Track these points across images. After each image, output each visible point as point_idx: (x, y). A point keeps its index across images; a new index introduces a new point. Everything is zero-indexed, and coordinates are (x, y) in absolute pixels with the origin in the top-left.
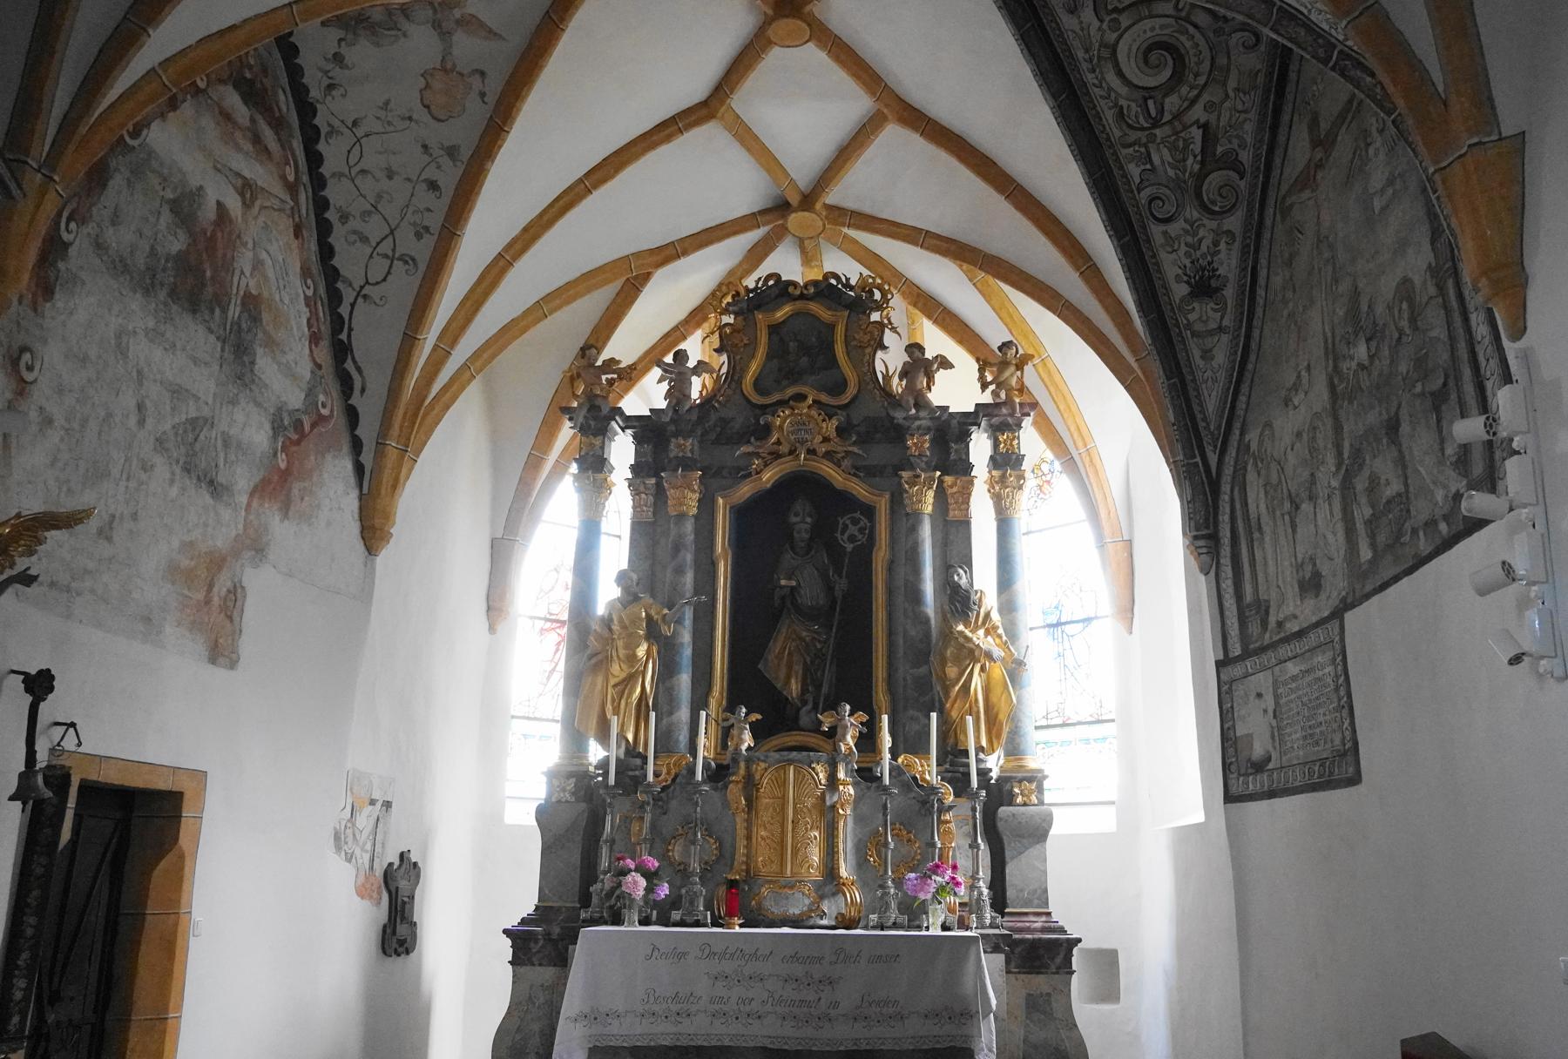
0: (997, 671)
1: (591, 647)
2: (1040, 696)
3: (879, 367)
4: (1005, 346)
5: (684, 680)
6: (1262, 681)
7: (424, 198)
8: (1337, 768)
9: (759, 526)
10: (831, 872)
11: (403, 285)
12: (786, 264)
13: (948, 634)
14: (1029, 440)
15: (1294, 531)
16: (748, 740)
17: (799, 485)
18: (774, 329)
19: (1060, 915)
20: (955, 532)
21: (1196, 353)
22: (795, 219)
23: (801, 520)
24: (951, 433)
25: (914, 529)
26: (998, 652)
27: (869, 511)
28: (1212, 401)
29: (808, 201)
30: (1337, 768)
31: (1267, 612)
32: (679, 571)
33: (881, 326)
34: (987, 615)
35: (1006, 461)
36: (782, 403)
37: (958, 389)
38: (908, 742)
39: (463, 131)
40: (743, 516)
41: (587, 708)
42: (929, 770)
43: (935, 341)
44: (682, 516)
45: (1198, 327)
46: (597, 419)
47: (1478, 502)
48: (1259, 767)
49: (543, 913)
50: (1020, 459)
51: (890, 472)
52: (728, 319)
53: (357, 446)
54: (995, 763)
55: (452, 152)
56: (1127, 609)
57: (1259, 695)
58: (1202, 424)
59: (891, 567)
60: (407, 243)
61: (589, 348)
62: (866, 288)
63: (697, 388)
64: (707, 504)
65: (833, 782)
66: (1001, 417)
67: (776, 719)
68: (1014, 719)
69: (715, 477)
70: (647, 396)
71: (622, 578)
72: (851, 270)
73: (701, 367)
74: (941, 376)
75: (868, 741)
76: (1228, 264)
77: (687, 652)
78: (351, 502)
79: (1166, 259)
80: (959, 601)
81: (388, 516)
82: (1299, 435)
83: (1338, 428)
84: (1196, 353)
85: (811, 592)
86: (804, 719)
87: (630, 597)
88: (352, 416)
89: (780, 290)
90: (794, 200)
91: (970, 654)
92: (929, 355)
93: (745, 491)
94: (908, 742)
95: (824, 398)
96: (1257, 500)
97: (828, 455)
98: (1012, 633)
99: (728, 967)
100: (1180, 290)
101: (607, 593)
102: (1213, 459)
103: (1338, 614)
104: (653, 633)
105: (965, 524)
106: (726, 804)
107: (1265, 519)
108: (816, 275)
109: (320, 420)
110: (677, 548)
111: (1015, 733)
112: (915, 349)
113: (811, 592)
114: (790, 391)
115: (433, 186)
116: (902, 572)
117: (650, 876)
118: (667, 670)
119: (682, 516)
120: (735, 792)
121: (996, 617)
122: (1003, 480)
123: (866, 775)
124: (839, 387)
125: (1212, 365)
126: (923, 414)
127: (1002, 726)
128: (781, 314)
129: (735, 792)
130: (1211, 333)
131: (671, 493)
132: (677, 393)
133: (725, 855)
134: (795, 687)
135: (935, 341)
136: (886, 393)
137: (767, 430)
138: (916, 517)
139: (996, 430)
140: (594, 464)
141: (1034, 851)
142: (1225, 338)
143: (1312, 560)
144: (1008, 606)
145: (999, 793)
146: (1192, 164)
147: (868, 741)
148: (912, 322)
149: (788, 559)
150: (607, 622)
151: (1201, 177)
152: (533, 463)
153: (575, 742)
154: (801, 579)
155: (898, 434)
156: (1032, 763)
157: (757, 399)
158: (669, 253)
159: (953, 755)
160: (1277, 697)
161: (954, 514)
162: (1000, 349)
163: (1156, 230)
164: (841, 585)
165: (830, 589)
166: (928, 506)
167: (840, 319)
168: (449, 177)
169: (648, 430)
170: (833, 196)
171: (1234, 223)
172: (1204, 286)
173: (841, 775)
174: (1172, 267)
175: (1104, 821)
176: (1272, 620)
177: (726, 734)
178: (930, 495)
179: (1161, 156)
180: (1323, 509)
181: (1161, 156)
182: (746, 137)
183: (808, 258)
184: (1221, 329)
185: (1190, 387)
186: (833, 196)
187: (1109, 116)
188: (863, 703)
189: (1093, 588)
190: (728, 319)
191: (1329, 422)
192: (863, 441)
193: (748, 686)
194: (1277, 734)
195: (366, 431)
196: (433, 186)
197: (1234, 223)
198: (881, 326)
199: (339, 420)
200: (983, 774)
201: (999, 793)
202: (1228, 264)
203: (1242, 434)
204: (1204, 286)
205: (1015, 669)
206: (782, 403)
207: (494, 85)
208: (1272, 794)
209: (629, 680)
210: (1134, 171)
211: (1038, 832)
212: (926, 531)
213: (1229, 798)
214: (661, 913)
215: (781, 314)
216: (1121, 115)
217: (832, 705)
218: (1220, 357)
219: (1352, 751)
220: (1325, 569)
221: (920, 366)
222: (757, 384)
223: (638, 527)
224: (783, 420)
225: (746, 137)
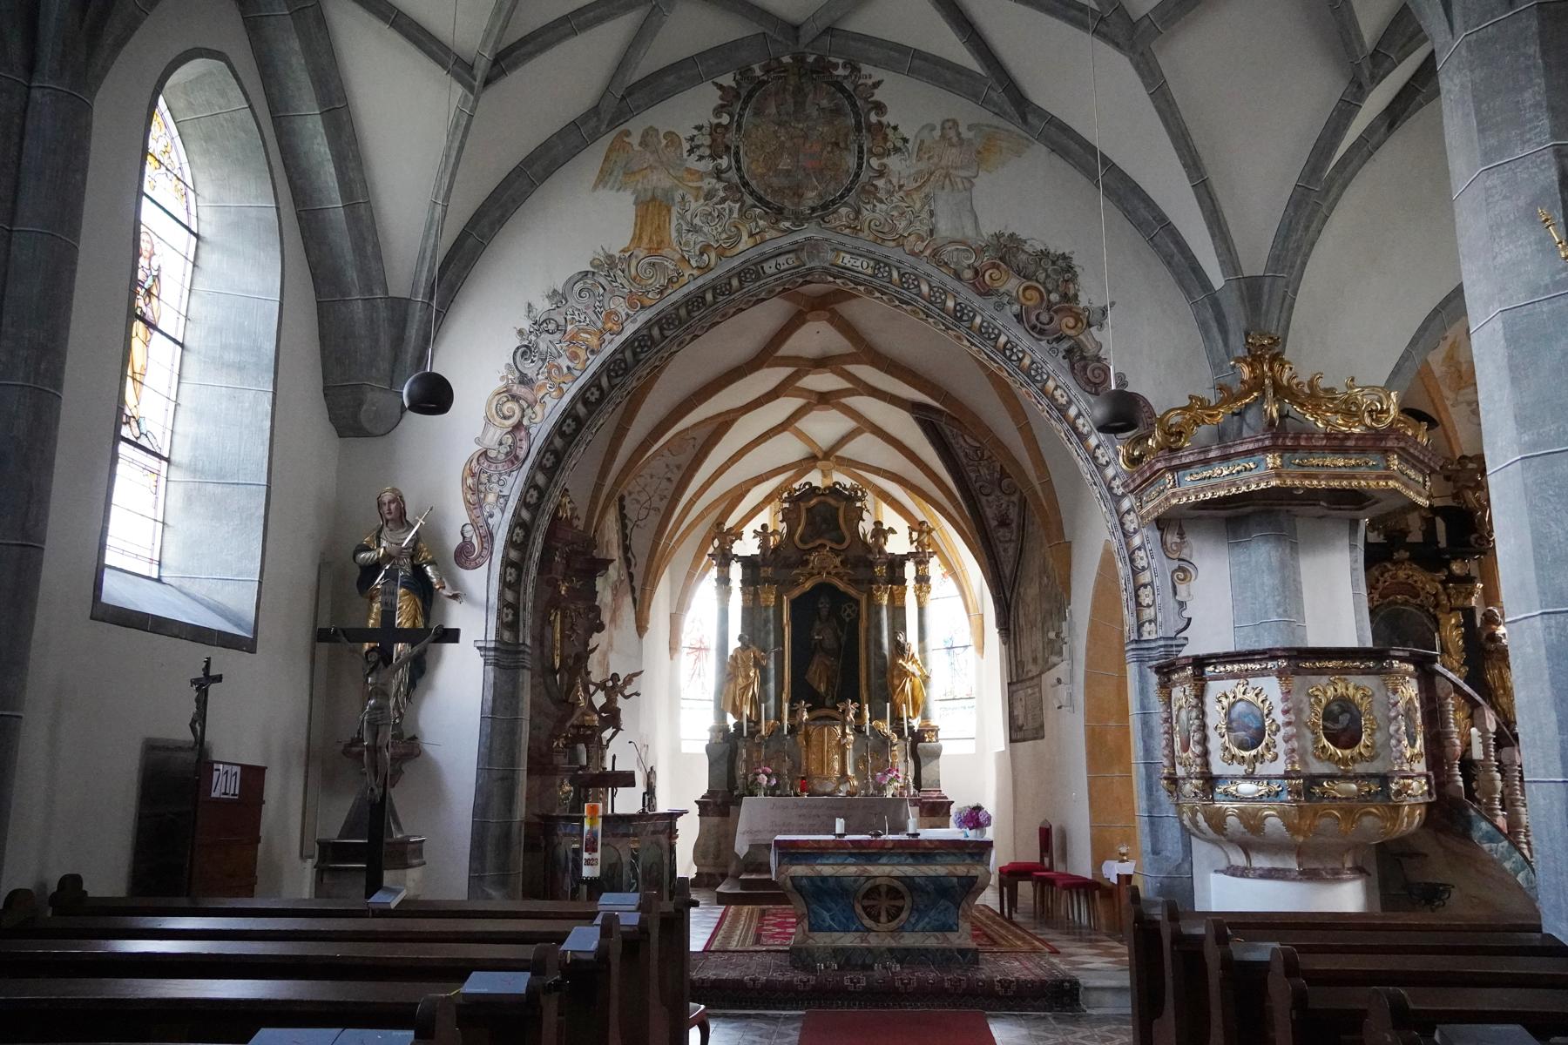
0: (918, 681)
1: (730, 671)
2: (936, 691)
3: (861, 530)
5: (772, 685)
7: (665, 483)
8: (1038, 733)
11: (655, 519)
12: (815, 478)
13: (895, 664)
14: (935, 567)
16: (806, 716)
17: (820, 589)
18: (809, 510)
19: (945, 792)
20: (898, 613)
22: (819, 464)
23: (824, 605)
24: (897, 562)
25: (878, 613)
26: (918, 673)
27: (857, 603)
29: (827, 455)
30: (1038, 733)
32: (768, 633)
33: (861, 509)
35: (922, 579)
37: (898, 544)
38: (878, 715)
39: (685, 459)
41: (726, 700)
42: (886, 727)
43: (890, 518)
44: (767, 607)
46: (725, 558)
47: (1054, 659)
48: (1020, 728)
49: (711, 792)
50: (928, 579)
51: (868, 583)
52: (786, 505)
53: (633, 590)
54: (916, 723)
55: (678, 467)
56: (981, 648)
59: (868, 630)
60: (656, 502)
61: (719, 523)
62: (853, 489)
63: (772, 541)
65: (844, 734)
66: (920, 559)
67: (816, 702)
68: (925, 702)
69: (783, 585)
70: (748, 546)
71: (740, 638)
72: (847, 482)
73: (775, 532)
74: (891, 537)
75: (859, 715)
76: (1013, 514)
77: (772, 672)
78: (633, 616)
79: (988, 510)
80: (900, 649)
81: (647, 621)
85: (829, 642)
86: (828, 703)
87: (745, 647)
88: (631, 576)
89: (813, 491)
90: (820, 455)
91: (905, 673)
92: (886, 527)
93: (796, 593)
94: (878, 715)
96: (1022, 621)
97: (837, 574)
98: (925, 663)
99: (804, 811)
100: (994, 523)
101: (734, 644)
103: (1042, 673)
104: (757, 664)
106: (796, 743)
108: (829, 482)
110: (766, 622)
111: (925, 710)
112: (878, 523)
113: (829, 642)
114: (818, 542)
115: (669, 480)
116: (873, 632)
117: (768, 776)
118: (764, 682)
119: (767, 607)
120: (800, 739)
121: (917, 656)
122: (920, 589)
123: (858, 730)
124: (841, 540)
125: (1007, 554)
127: (920, 706)
128: (813, 502)
129: (800, 739)
131: (763, 596)
132: (763, 546)
133: (796, 766)
134: (822, 689)
135: (890, 518)
136: (865, 543)
137: (806, 563)
138: (880, 606)
139: (918, 564)
140: (724, 580)
144: (923, 650)
145: (918, 737)
146: (997, 475)
147: (859, 715)
148: (876, 503)
149: (817, 625)
150: (734, 658)
151: (1000, 481)
152: (690, 576)
153: (721, 716)
154: (823, 634)
155: (871, 565)
156: (933, 723)
157: (801, 546)
158: (759, 480)
159: (897, 720)
161: (898, 603)
163: (984, 499)
164: (844, 639)
165: (838, 639)
166: (885, 600)
167: (842, 506)
168: (676, 477)
169: (747, 562)
170: (839, 453)
171: (1015, 498)
172: (1004, 522)
174: (990, 513)
175: (969, 748)
177: (793, 713)
178: (886, 597)
179: (984, 471)
181: (984, 471)
182: (800, 435)
183: (825, 475)
186: (839, 453)
187: (962, 455)
188: (856, 698)
189: (965, 635)
190: (786, 505)
192: (855, 566)
193: (802, 691)
194: (1026, 716)
195: (637, 583)
196: (669, 480)
197: (1015, 498)
198: (861, 509)
199: (627, 580)
200: (911, 728)
201: (918, 737)
202: (1013, 514)
204: (1004, 522)
205: (926, 680)
207: (700, 442)
209: (746, 688)
210: (973, 475)
211: (936, 754)
213: (1012, 741)
214: (771, 791)
215: (813, 502)
216: (966, 455)
217: (843, 700)
218: (1011, 552)
219: (1042, 726)
222: (801, 539)
223: (745, 610)
224: (814, 558)
225: (800, 435)
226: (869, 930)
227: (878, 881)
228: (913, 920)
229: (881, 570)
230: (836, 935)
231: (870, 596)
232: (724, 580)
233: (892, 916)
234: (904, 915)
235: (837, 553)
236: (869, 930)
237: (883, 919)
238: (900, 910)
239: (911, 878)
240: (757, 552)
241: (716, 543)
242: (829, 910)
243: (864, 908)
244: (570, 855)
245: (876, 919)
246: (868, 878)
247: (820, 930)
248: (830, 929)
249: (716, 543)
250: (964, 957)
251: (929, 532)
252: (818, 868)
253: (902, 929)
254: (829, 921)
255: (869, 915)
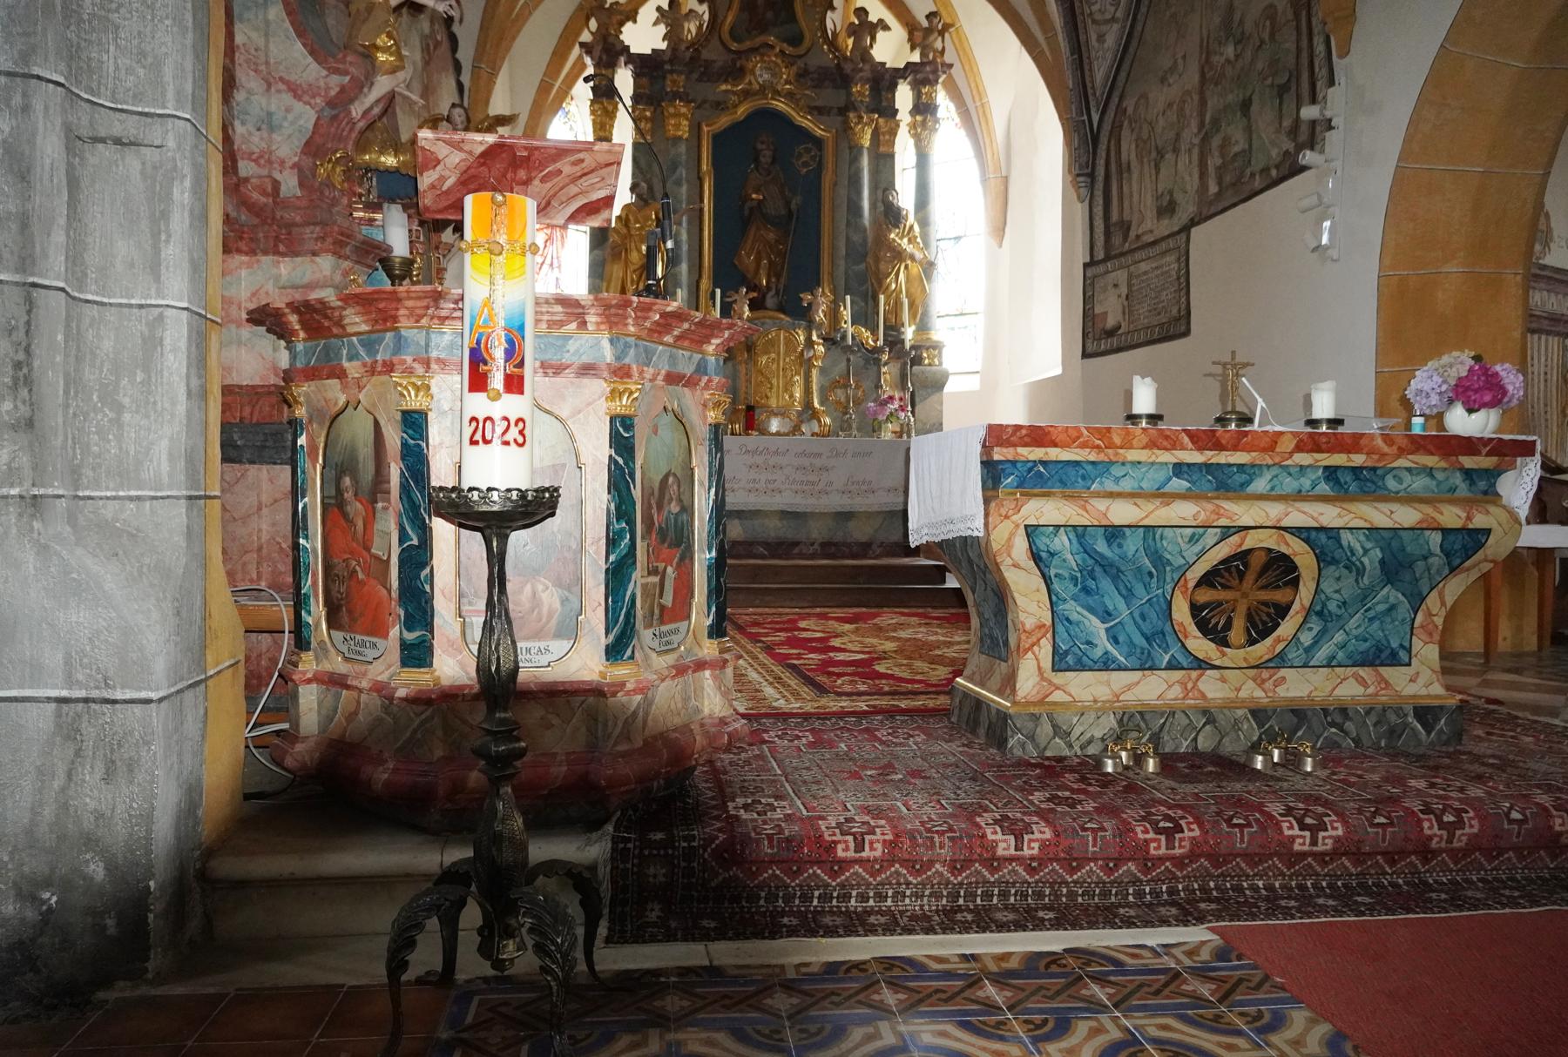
0: (915, 269)
4: (931, 16)
6: (1121, 276)
9: (735, 149)
10: (808, 404)
15: (1157, 173)
20: (883, 162)
21: (1094, 37)
24: (884, 80)
25: (855, 159)
26: (919, 255)
28: (1100, 72)
31: (1129, 229)
34: (911, 227)
35: (924, 109)
36: (754, 50)
37: (890, 48)
40: (719, 140)
45: (1098, 17)
48: (1111, 333)
56: (999, 229)
57: (1116, 286)
58: (1090, 91)
64: (696, 129)
65: (810, 343)
66: (923, 75)
74: (880, 35)
75: (834, 315)
80: (892, 215)
82: (1170, 105)
83: (1203, 102)
84: (1094, 37)
91: (899, 255)
93: (724, 121)
95: (789, 50)
102: (1096, 118)
103: (1186, 229)
105: (891, 157)
107: (1134, 164)
109: (437, 44)
111: (925, 314)
114: (759, 40)
124: (796, 40)
126: (867, 67)
130: (1107, 22)
138: (855, 151)
139: (917, 86)
141: (935, 398)
142: (1116, 27)
143: (1171, 193)
144: (924, 222)
157: (734, 46)
159: (893, 329)
160: (1130, 286)
162: (927, 17)
166: (867, 144)
169: (646, 66)
173: (814, 338)
175: (973, 383)
176: (1132, 234)
178: (868, 136)
180: (1184, 159)
184: (1113, 19)
185: (1086, 61)
191: (1196, 97)
194: (1128, 310)
195: (466, 54)
199: (446, 45)
203: (1121, 98)
205: (929, 267)
206: (754, 50)
208: (1119, 350)
211: (937, 384)
212: (865, 161)
213: (1086, 355)
218: (1110, 41)
220: (1179, 197)
221: (865, 28)
226: (1202, 665)
227: (1251, 541)
228: (1306, 638)
229: (861, 90)
230: (1120, 679)
231: (846, 131)
232: (604, 93)
233: (1261, 627)
234: (1286, 628)
235: (790, 60)
236: (1202, 665)
237: (1237, 634)
238: (1283, 611)
239: (1332, 533)
240: (663, 46)
241: (593, 24)
242: (1106, 615)
243: (1195, 609)
244: (394, 438)
245: (1220, 638)
246: (1227, 532)
247: (1080, 667)
248: (1107, 665)
249: (593, 24)
250: (1428, 728)
251: (941, 34)
252: (1101, 505)
253: (1279, 661)
254: (1104, 644)
255: (1204, 627)
